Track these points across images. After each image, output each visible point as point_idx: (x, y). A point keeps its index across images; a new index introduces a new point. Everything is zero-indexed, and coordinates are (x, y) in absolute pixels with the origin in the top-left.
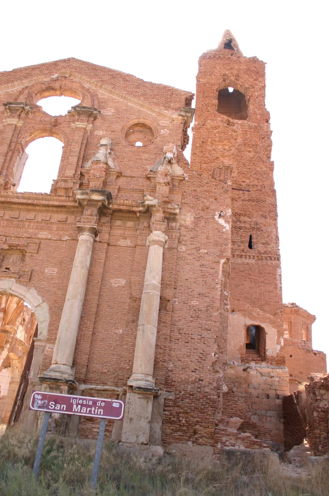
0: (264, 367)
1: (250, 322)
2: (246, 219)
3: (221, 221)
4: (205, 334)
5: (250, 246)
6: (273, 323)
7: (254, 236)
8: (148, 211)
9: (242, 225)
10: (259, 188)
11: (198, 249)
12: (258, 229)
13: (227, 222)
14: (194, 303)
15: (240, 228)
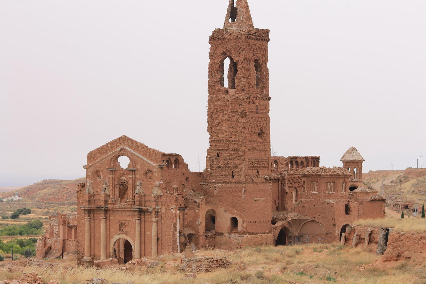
0: (237, 236)
1: (232, 216)
2: (231, 161)
3: (172, 210)
4: (169, 247)
5: (233, 176)
6: (240, 216)
7: (234, 172)
8: (151, 212)
9: (230, 165)
10: (237, 142)
11: (167, 220)
12: (236, 167)
13: (174, 210)
14: (166, 238)
15: (229, 167)
